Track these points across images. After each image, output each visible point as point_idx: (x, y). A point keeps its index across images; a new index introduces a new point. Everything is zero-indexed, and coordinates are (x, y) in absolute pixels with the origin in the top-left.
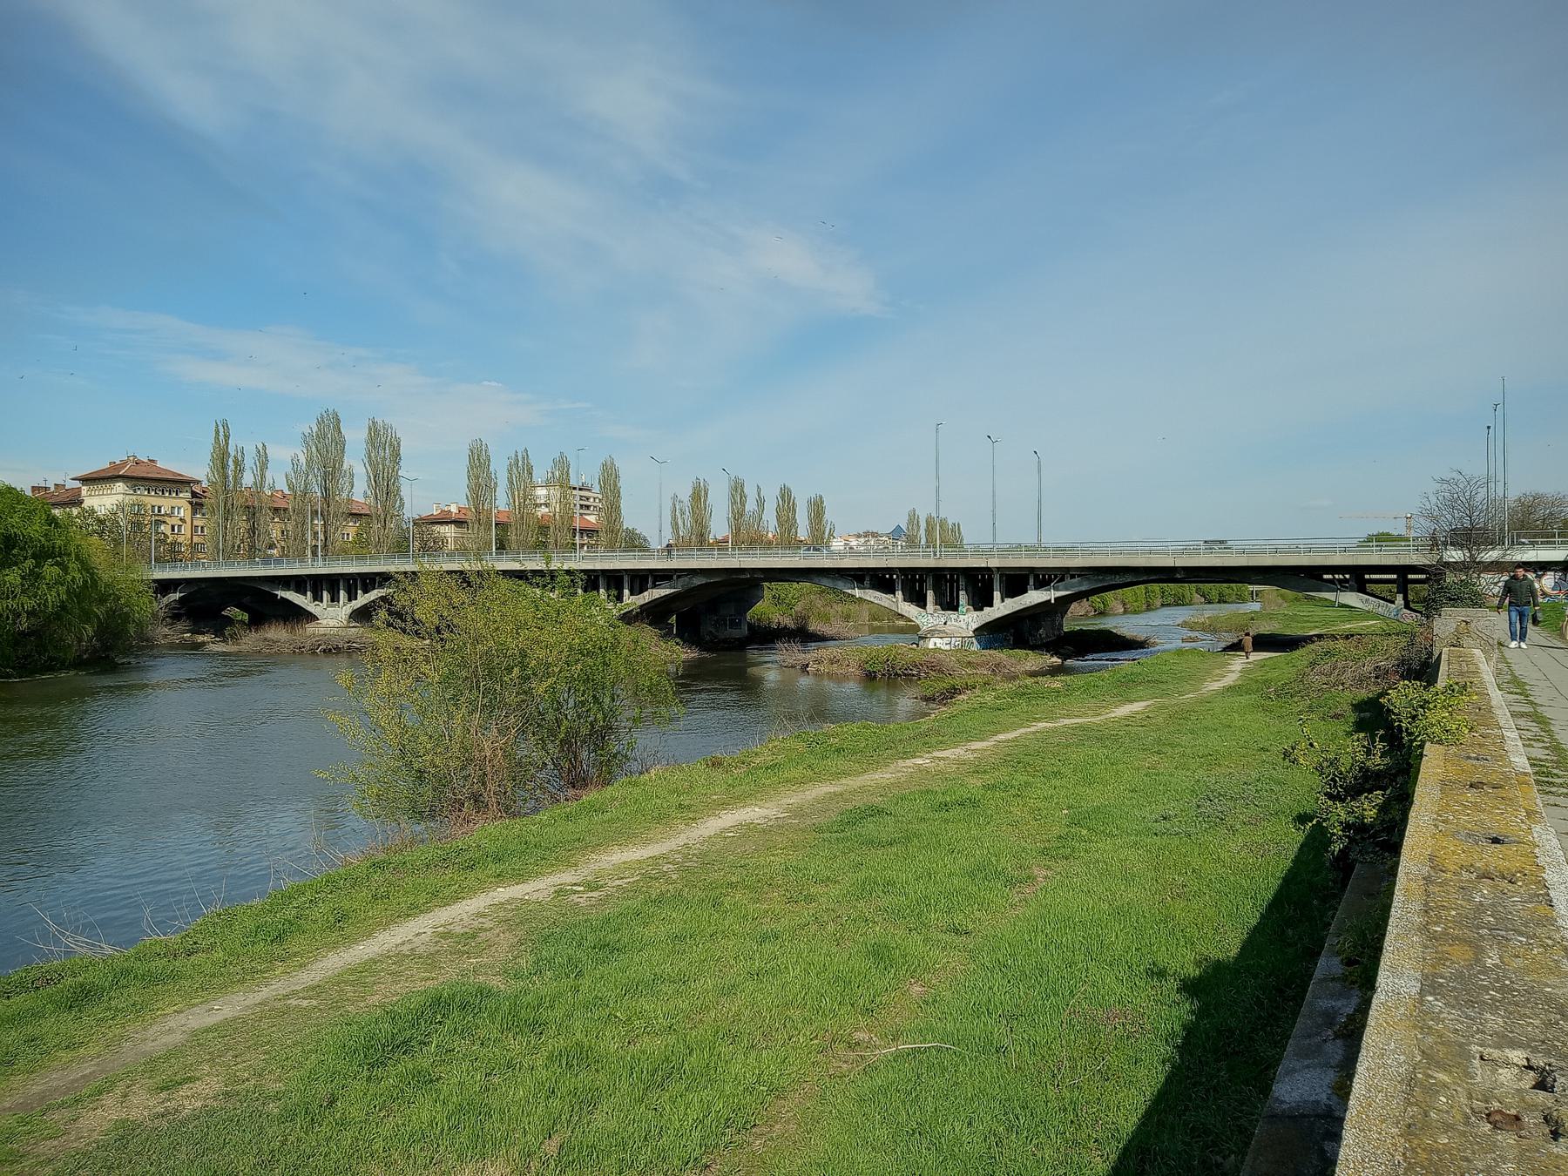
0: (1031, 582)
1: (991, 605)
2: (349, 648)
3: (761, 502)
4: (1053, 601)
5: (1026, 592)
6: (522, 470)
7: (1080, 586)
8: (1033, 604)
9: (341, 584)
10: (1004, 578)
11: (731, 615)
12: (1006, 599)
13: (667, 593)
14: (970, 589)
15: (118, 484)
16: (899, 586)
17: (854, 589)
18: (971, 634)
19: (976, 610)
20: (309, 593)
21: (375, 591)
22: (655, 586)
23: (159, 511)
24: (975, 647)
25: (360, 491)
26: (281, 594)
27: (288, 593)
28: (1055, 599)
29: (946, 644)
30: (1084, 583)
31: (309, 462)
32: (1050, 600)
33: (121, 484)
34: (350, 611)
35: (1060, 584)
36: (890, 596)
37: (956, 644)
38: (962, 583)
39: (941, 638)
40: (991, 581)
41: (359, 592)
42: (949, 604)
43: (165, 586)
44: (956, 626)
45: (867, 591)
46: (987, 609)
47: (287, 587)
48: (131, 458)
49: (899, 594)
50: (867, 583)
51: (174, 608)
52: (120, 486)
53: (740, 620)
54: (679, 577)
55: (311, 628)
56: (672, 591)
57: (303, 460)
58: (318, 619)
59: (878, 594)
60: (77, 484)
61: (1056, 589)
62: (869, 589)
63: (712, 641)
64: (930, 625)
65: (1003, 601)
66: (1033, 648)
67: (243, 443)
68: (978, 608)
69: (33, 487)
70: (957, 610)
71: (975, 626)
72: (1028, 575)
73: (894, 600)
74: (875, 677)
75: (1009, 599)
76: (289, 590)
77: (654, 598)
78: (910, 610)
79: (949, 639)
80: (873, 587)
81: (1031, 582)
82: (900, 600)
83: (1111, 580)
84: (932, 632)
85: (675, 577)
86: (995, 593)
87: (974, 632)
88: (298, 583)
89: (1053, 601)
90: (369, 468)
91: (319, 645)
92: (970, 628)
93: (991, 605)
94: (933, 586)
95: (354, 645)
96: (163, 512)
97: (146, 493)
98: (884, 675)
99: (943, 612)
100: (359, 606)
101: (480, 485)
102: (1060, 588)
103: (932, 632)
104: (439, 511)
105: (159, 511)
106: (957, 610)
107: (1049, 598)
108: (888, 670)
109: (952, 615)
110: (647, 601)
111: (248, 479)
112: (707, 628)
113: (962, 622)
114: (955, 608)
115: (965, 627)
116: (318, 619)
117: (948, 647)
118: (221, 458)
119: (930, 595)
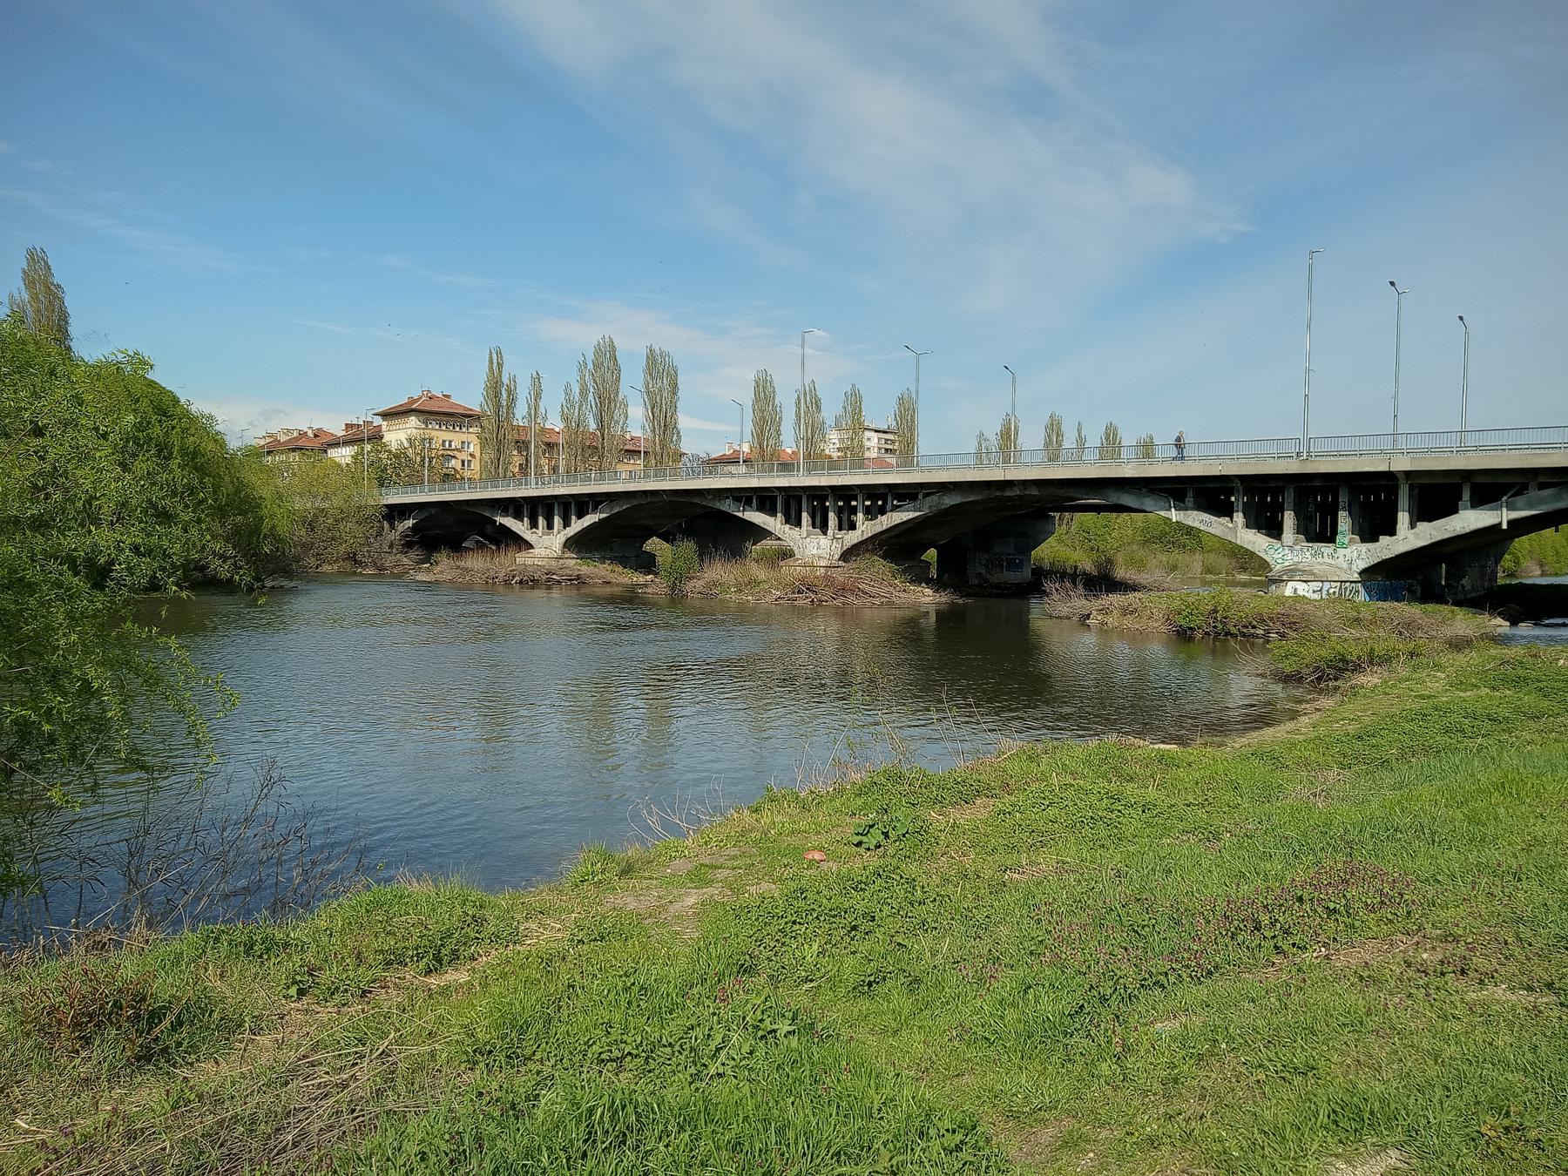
0: (1466, 495)
1: (1392, 532)
2: (549, 580)
3: (1081, 441)
4: (1505, 526)
5: (1456, 511)
6: (810, 403)
7: (1558, 501)
8: (1467, 530)
9: (556, 508)
10: (1416, 492)
11: (1009, 554)
13: (911, 517)
14: (1355, 509)
15: (411, 418)
17: (1169, 509)
18: (1356, 577)
19: (1363, 541)
21: (588, 517)
22: (895, 508)
23: (450, 445)
24: (1362, 596)
25: (636, 422)
26: (500, 520)
27: (506, 519)
28: (1509, 522)
29: (1314, 592)
31: (584, 393)
32: (1500, 524)
33: (413, 418)
34: (563, 539)
35: (1518, 498)
37: (1331, 591)
38: (1343, 498)
40: (1393, 492)
41: (573, 517)
42: (1320, 532)
43: (395, 513)
46: (1384, 540)
47: (505, 513)
48: (425, 393)
49: (1239, 518)
50: (1189, 501)
51: (407, 536)
52: (413, 421)
53: (1021, 561)
54: (927, 495)
55: (522, 558)
56: (917, 514)
57: (576, 389)
58: (531, 547)
59: (1206, 516)
60: (378, 421)
61: (1511, 508)
62: (1192, 509)
63: (980, 585)
64: (1287, 564)
65: (1412, 526)
67: (518, 371)
69: (346, 424)
71: (1363, 565)
72: (1461, 484)
73: (1230, 525)
74: (1191, 639)
75: (1425, 524)
76: (507, 516)
77: (893, 524)
78: (1255, 541)
79: (1320, 584)
80: (1200, 507)
81: (1466, 495)
82: (1240, 526)
84: (1292, 573)
85: (920, 496)
86: (1400, 515)
87: (1360, 574)
88: (515, 507)
89: (1505, 526)
90: (646, 400)
91: (514, 577)
92: (1354, 567)
93: (1392, 532)
95: (554, 577)
96: (453, 447)
97: (437, 427)
98: (1207, 634)
99: (1311, 545)
100: (572, 534)
101: (766, 421)
102: (1518, 505)
104: (732, 451)
105: (450, 445)
107: (1496, 521)
108: (1215, 627)
109: (1326, 548)
110: (884, 528)
111: (521, 410)
112: (977, 569)
115: (1345, 566)
116: (531, 547)
117: (1316, 596)
118: (495, 386)
119: (1289, 519)
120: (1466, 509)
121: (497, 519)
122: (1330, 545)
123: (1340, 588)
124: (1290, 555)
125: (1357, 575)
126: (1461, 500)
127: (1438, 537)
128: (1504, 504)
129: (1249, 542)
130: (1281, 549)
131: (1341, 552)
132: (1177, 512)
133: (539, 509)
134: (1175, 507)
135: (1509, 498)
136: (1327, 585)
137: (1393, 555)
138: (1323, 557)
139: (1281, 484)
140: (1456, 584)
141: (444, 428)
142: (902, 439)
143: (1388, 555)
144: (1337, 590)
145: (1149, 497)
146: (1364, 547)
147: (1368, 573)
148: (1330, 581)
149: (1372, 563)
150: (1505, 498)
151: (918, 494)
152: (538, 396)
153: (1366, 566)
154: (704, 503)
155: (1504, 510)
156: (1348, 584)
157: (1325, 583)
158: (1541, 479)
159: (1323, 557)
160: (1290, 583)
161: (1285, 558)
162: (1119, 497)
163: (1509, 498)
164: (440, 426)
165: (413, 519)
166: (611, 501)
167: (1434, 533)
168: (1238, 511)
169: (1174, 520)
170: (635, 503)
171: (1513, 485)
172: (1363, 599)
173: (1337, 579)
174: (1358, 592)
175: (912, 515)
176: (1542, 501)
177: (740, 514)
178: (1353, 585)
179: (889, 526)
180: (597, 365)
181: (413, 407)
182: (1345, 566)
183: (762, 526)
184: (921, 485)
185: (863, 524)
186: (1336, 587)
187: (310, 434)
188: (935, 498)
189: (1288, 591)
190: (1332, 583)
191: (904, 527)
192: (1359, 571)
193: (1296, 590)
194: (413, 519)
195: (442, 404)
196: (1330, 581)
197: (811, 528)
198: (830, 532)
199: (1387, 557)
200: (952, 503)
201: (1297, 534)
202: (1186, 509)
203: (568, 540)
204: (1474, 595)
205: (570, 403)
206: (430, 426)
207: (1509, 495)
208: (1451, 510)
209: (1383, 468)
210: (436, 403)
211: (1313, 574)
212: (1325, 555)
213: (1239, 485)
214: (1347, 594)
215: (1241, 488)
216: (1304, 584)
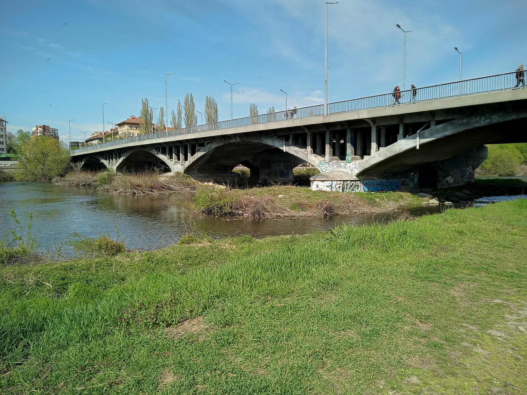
0: (401, 131)
1: (369, 154)
4: (418, 148)
7: (445, 131)
8: (402, 151)
13: (203, 154)
16: (309, 142)
17: (283, 146)
18: (355, 178)
20: (108, 160)
22: (199, 150)
24: (361, 189)
29: (327, 186)
30: (449, 128)
31: (180, 113)
32: (415, 147)
33: (126, 126)
35: (426, 131)
36: (303, 150)
40: (369, 130)
43: (76, 159)
45: (291, 147)
46: (366, 157)
49: (309, 148)
50: (290, 141)
52: (126, 127)
53: (288, 173)
54: (209, 143)
56: (205, 153)
57: (176, 113)
59: (296, 149)
60: (117, 127)
61: (422, 137)
71: (357, 171)
73: (306, 153)
79: (331, 182)
81: (401, 131)
83: (476, 122)
85: (205, 144)
86: (372, 144)
92: (353, 173)
93: (369, 154)
97: (135, 129)
109: (342, 163)
110: (196, 159)
113: (348, 168)
117: (328, 190)
119: (328, 148)
120: (400, 139)
121: (101, 160)
125: (355, 177)
126: (399, 134)
128: (418, 135)
132: (286, 147)
133: (110, 154)
134: (285, 145)
135: (420, 131)
137: (369, 166)
138: (341, 168)
139: (324, 130)
141: (138, 129)
142: (212, 120)
143: (367, 166)
144: (341, 185)
145: (276, 140)
147: (364, 175)
149: (361, 171)
150: (418, 131)
151: (204, 143)
152: (162, 116)
153: (359, 172)
154: (148, 151)
155: (418, 138)
156: (348, 182)
157: (333, 182)
158: (438, 118)
159: (341, 168)
160: (315, 182)
162: (266, 141)
163: (420, 131)
164: (136, 129)
165: (84, 161)
166: (127, 152)
169: (285, 151)
170: (134, 151)
171: (424, 123)
173: (340, 180)
175: (203, 153)
176: (437, 132)
177: (157, 155)
178: (352, 182)
179: (197, 158)
180: (186, 104)
181: (125, 122)
183: (162, 160)
184: (204, 139)
185: (190, 158)
187: (103, 133)
188: (209, 145)
190: (338, 182)
191: (205, 159)
192: (356, 175)
193: (317, 186)
194: (84, 161)
195: (137, 120)
196: (337, 181)
197: (177, 160)
198: (181, 162)
199: (367, 167)
200: (214, 147)
202: (289, 146)
203: (117, 168)
205: (174, 119)
206: (133, 129)
207: (421, 129)
210: (135, 120)
212: (342, 167)
214: (348, 187)
216: (321, 182)
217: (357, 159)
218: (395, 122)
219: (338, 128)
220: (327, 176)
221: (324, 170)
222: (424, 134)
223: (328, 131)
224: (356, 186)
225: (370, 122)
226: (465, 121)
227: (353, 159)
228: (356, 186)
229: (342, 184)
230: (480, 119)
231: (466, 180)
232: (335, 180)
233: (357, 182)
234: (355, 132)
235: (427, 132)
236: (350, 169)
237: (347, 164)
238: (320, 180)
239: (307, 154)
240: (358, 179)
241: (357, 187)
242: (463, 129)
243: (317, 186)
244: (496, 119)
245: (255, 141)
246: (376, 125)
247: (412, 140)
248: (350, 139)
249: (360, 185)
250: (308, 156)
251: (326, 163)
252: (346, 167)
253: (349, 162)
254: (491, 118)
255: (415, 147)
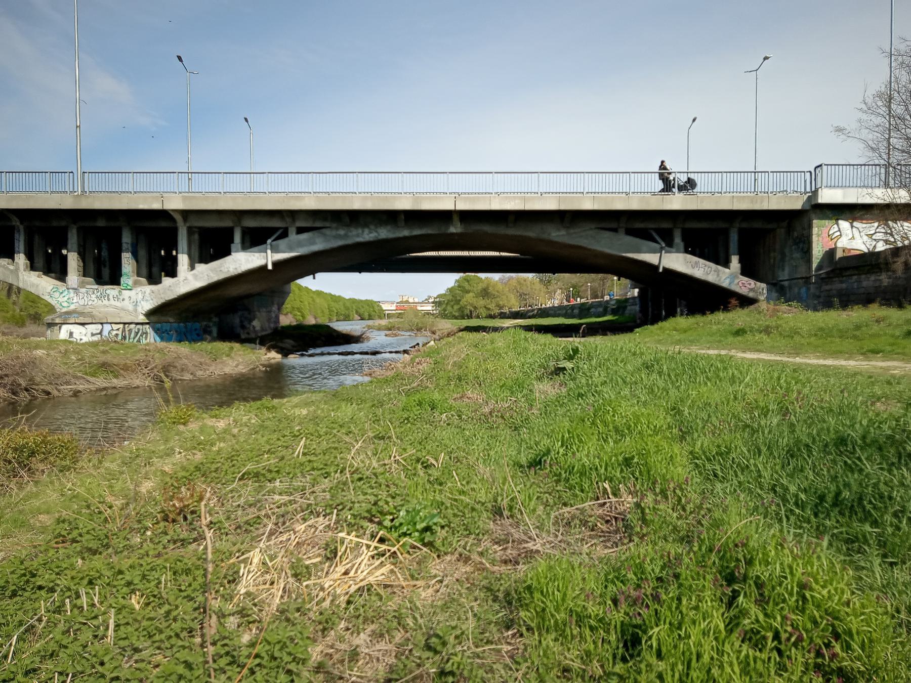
1: (173, 273)
4: (270, 267)
10: (196, 237)
12: (197, 265)
14: (142, 253)
16: (20, 244)
18: (142, 318)
24: (151, 337)
29: (93, 335)
30: (317, 240)
32: (266, 266)
38: (127, 238)
39: (83, 324)
40: (174, 232)
44: (116, 307)
46: (167, 281)
49: (21, 259)
61: (275, 250)
65: (192, 267)
66: (242, 341)
68: (153, 280)
70: (118, 284)
71: (148, 306)
73: (11, 267)
79: (100, 326)
82: (22, 267)
83: (358, 236)
84: (67, 317)
89: (270, 267)
92: (140, 309)
93: (173, 273)
94: (79, 246)
99: (96, 287)
103: (67, 317)
106: (118, 284)
109: (112, 290)
113: (127, 302)
114: (114, 279)
115: (131, 308)
119: (73, 261)
122: (115, 287)
123: (124, 331)
124: (75, 298)
126: (233, 242)
127: (215, 278)
128: (269, 246)
129: (33, 285)
130: (66, 292)
131: (126, 293)
135: (273, 241)
136: (107, 328)
138: (109, 300)
139: (63, 223)
140: (248, 326)
143: (171, 296)
144: (120, 332)
146: (149, 289)
147: (158, 314)
148: (111, 323)
150: (269, 241)
155: (269, 251)
156: (132, 326)
157: (104, 325)
161: (71, 301)
163: (273, 241)
167: (212, 275)
168: (19, 253)
171: (276, 229)
172: (153, 340)
173: (119, 321)
174: (146, 333)
176: (300, 244)
178: (138, 326)
182: (131, 308)
186: (118, 330)
189: (63, 334)
190: (113, 325)
192: (144, 312)
193: (71, 334)
196: (111, 323)
201: (84, 276)
204: (264, 333)
208: (226, 252)
209: (156, 206)
211: (92, 316)
212: (111, 297)
213: (18, 224)
214: (132, 335)
215: (21, 228)
217: (141, 284)
218: (227, 223)
219: (101, 223)
220: (90, 315)
221: (65, 304)
222: (277, 246)
223: (75, 227)
224: (144, 333)
225: (178, 218)
226: (342, 232)
227: (136, 283)
228: (144, 333)
229: (121, 330)
230: (363, 232)
231: (272, 325)
232: (109, 321)
233: (144, 326)
234: (137, 233)
235: (282, 243)
236: (132, 301)
237: (123, 291)
238: (77, 321)
239: (17, 269)
240: (147, 321)
241: (144, 336)
242: (340, 243)
243: (71, 334)
244: (384, 233)
245: (532, 232)
246: (188, 225)
247: (257, 255)
248: (129, 246)
249: (148, 331)
250: (20, 274)
251: (71, 290)
252: (121, 298)
253: (129, 287)
254: (377, 232)
255: (266, 266)
